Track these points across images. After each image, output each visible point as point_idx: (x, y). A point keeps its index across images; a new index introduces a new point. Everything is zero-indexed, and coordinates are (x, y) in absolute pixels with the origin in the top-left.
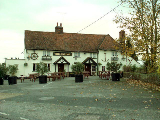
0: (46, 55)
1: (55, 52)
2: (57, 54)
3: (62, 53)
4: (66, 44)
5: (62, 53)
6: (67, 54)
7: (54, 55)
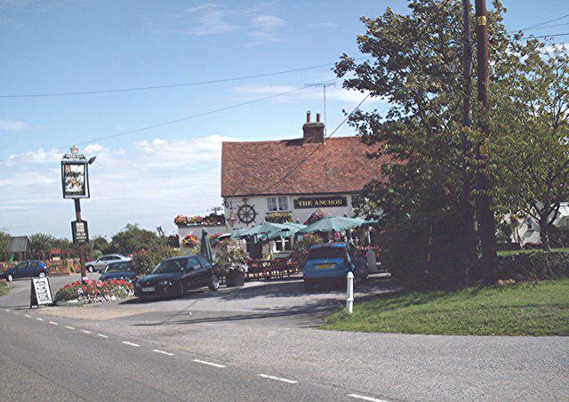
0: (275, 209)
1: (300, 200)
2: (305, 203)
3: (318, 199)
4: (330, 171)
5: (318, 199)
6: (333, 202)
7: (297, 206)
